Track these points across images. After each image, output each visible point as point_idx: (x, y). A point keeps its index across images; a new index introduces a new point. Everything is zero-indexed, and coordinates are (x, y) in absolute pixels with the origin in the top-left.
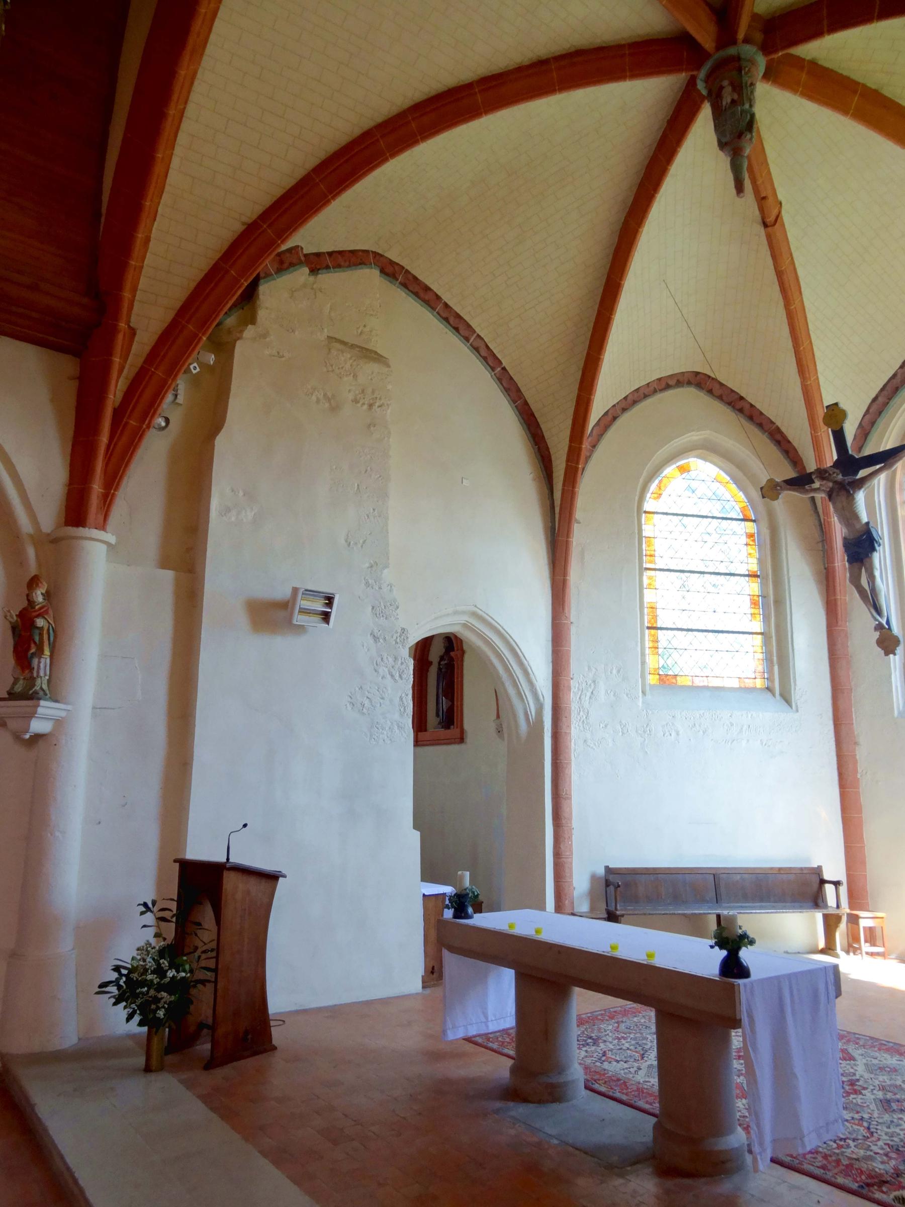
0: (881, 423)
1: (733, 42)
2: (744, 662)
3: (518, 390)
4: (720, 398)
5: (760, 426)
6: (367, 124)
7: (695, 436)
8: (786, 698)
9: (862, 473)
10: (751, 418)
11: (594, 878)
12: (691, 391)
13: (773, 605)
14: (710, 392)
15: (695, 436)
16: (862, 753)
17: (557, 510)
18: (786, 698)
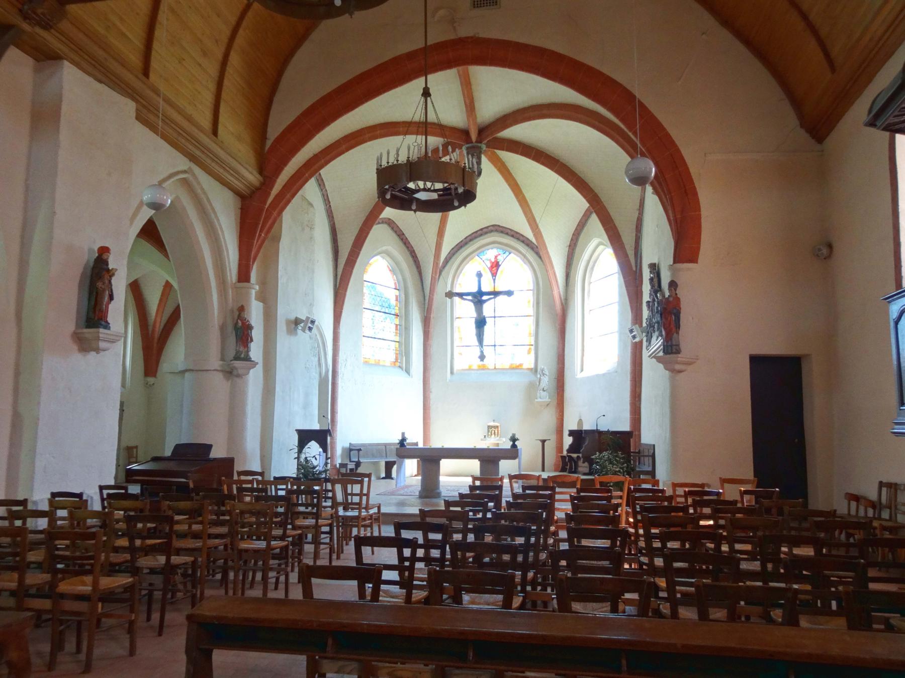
0: (452, 260)
1: (481, 142)
2: (388, 352)
3: (333, 217)
4: (396, 232)
5: (408, 248)
6: (364, 126)
7: (384, 248)
8: (408, 371)
9: (485, 298)
10: (405, 244)
11: (344, 449)
12: (385, 226)
13: (404, 330)
14: (392, 228)
15: (384, 248)
16: (433, 396)
17: (339, 277)
18: (408, 371)
